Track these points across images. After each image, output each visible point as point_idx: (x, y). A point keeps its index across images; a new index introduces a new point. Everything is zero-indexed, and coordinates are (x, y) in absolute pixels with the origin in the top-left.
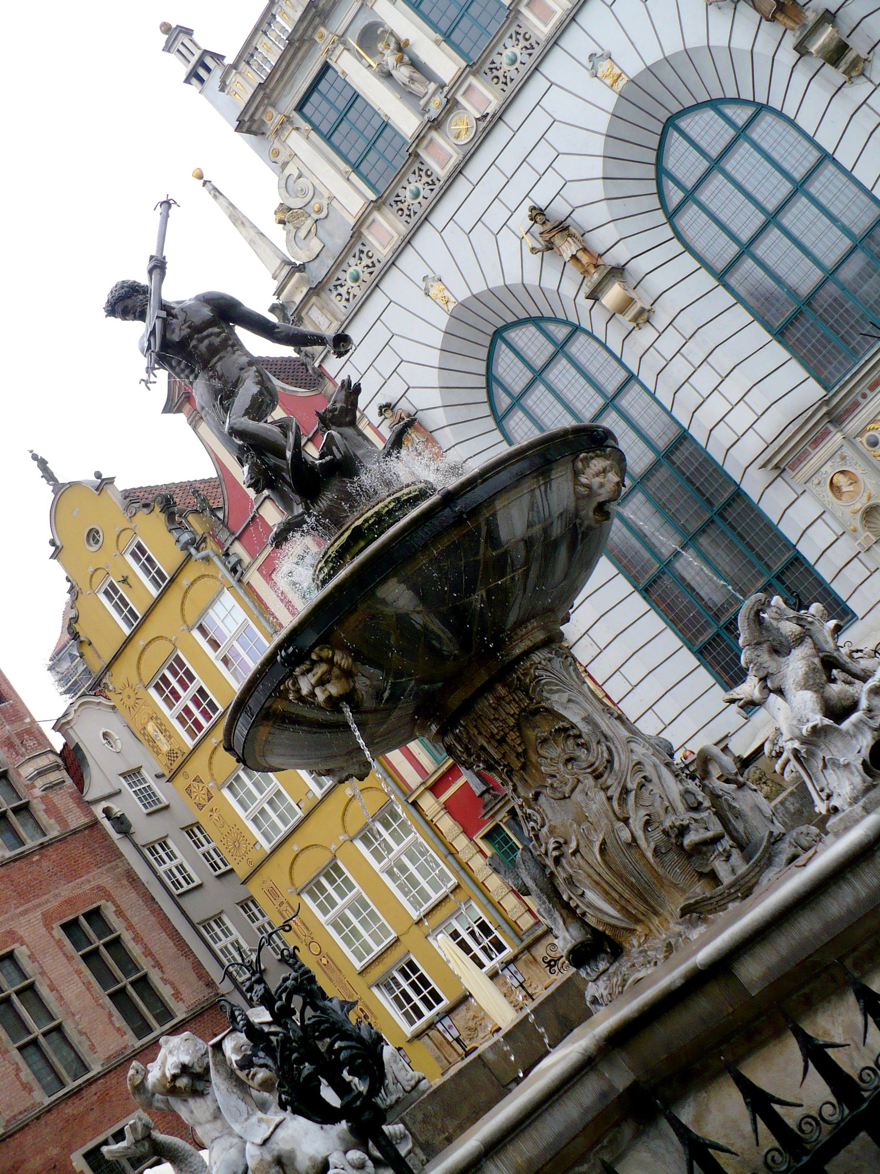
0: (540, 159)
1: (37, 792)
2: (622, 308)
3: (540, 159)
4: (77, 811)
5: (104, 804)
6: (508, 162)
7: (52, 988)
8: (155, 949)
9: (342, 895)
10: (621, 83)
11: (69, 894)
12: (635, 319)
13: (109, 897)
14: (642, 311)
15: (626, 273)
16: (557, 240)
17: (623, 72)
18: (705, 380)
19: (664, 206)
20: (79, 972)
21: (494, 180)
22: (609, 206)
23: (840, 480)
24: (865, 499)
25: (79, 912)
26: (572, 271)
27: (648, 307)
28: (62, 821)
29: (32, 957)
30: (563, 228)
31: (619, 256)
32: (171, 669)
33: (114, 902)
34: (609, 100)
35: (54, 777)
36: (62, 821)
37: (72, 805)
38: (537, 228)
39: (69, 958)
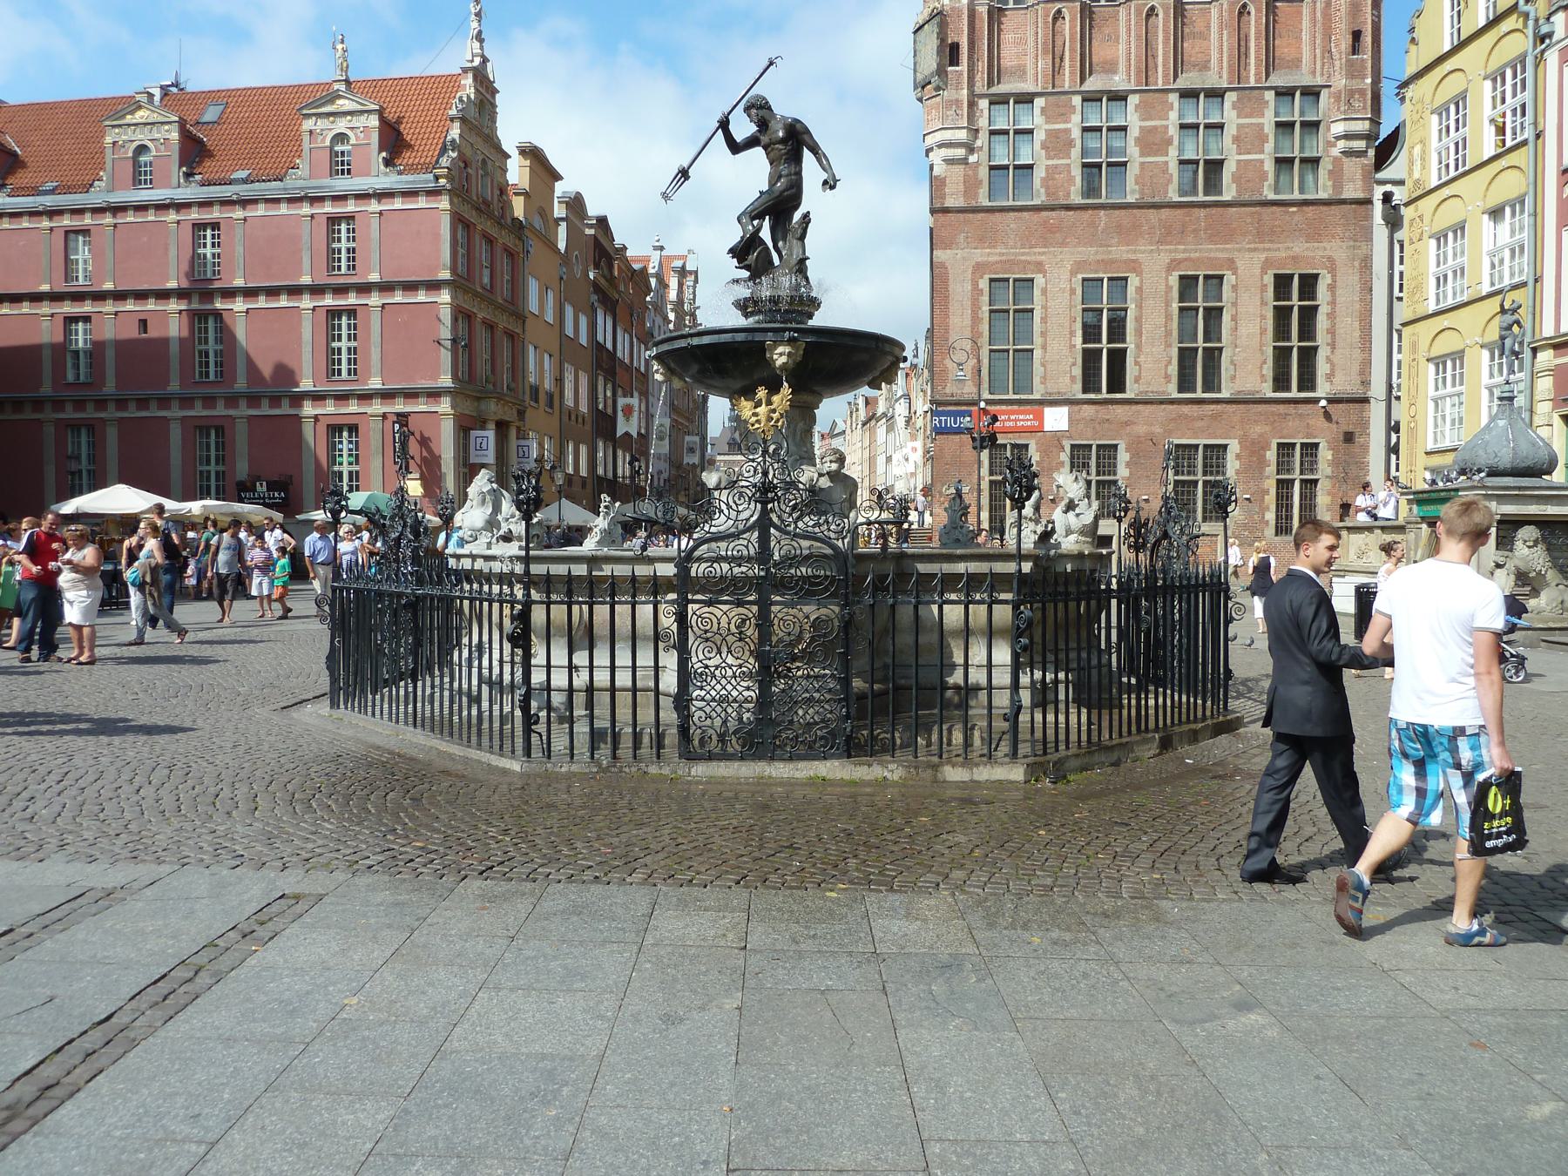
1: (1335, 152)
4: (1359, 183)
5: (1388, 188)
7: (1234, 318)
8: (1340, 331)
9: (1454, 385)
11: (1298, 253)
13: (1333, 271)
20: (1263, 317)
25: (1296, 271)
28: (1338, 186)
29: (1235, 288)
32: (1457, 105)
33: (1334, 276)
35: (1360, 145)
36: (1338, 186)
37: (1359, 176)
39: (1264, 303)
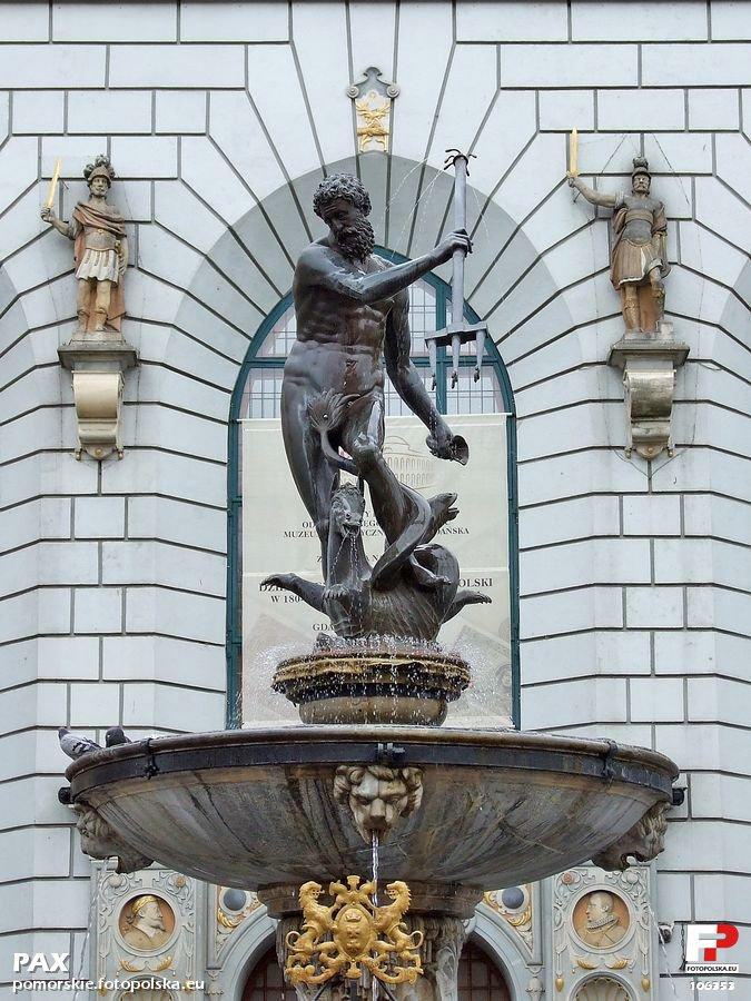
0: (178, 112)
2: (86, 415)
3: (178, 112)
6: (132, 66)
10: (375, 145)
12: (88, 443)
14: (109, 442)
15: (135, 374)
16: (95, 237)
17: (391, 135)
18: (97, 610)
19: (257, 340)
21: (86, 66)
22: (200, 270)
23: (148, 909)
24: (155, 964)
26: (66, 297)
27: (119, 446)
30: (117, 230)
31: (151, 343)
34: (339, 147)
38: (78, 191)
